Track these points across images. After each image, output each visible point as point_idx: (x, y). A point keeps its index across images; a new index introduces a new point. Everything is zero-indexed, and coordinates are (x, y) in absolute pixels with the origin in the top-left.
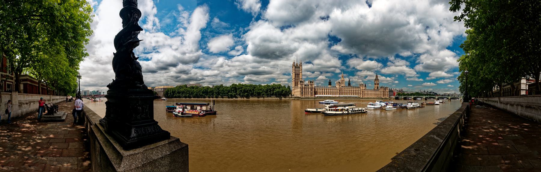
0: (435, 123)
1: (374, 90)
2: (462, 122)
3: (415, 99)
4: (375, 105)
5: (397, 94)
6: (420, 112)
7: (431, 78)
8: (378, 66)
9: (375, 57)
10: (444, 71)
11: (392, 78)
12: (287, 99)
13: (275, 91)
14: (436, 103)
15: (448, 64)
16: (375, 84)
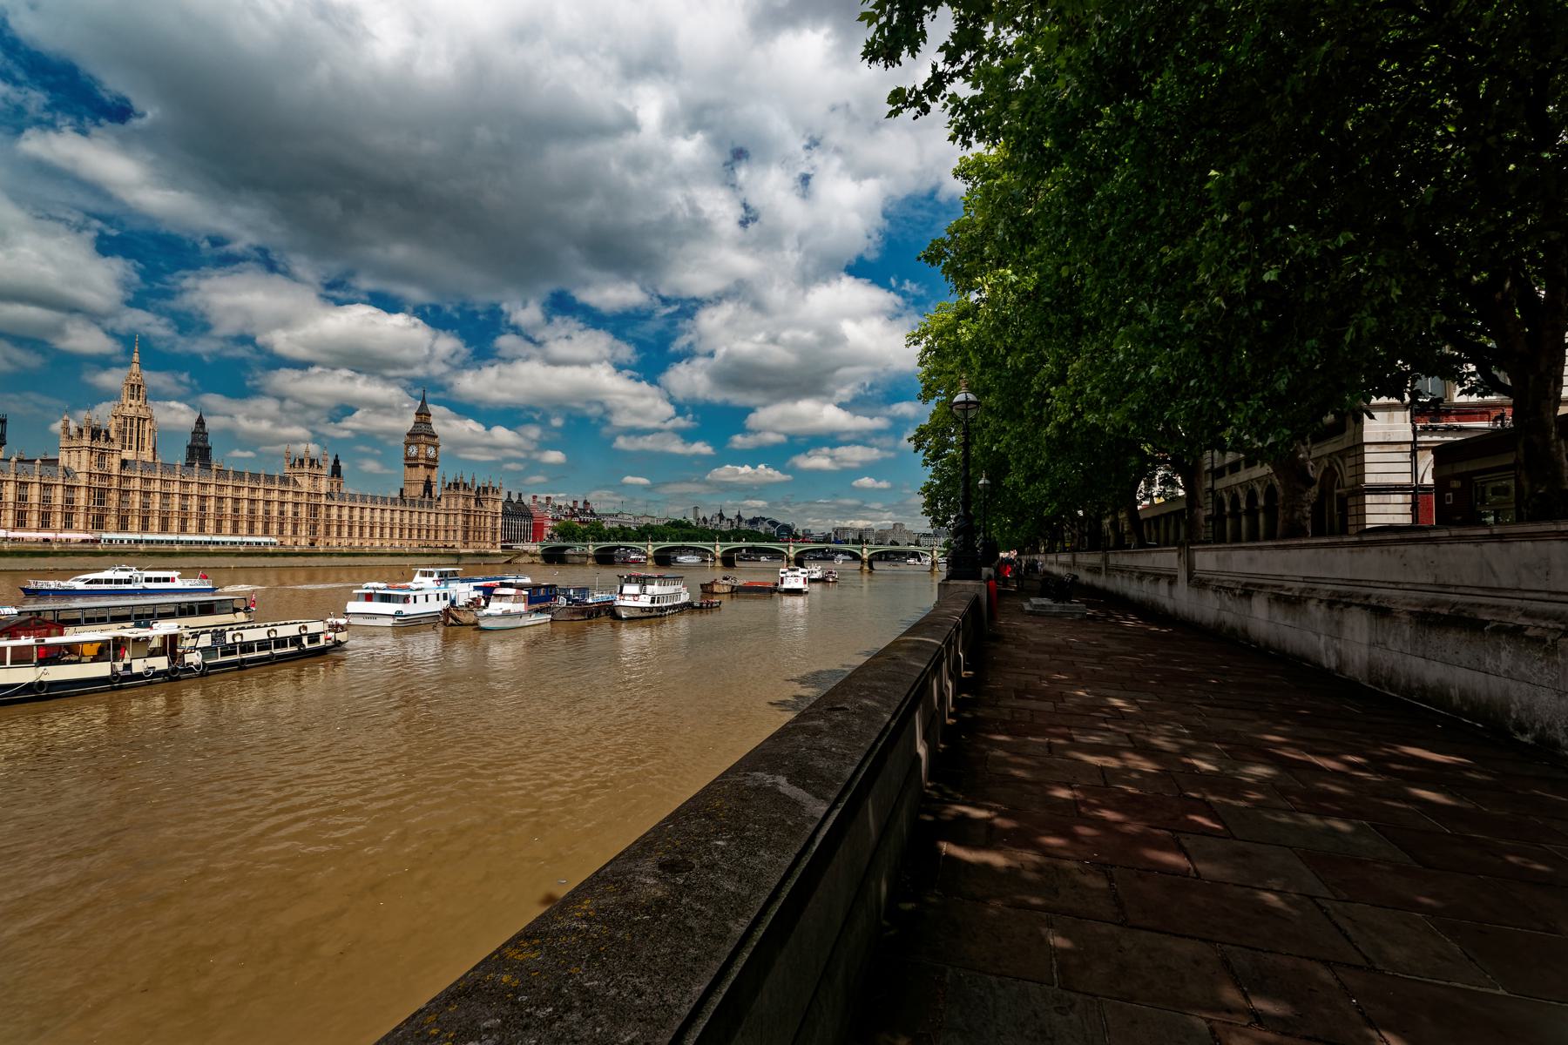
0: (782, 704)
1: (404, 502)
2: (942, 697)
3: (663, 559)
4: (406, 599)
6: (693, 640)
7: (760, 436)
8: (431, 349)
9: (415, 294)
10: (836, 399)
11: (523, 429)
14: (786, 586)
15: (855, 360)
16: (410, 466)
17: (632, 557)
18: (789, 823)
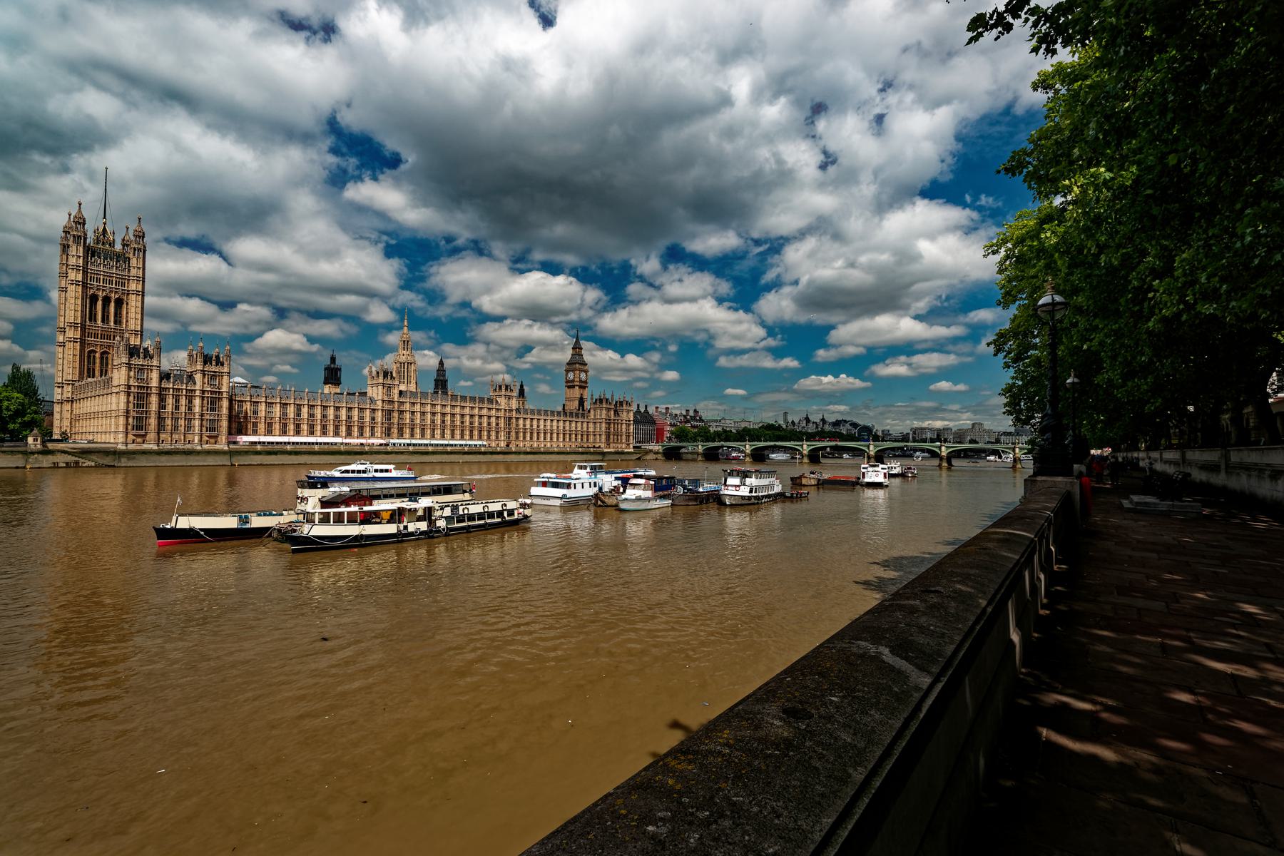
0: (867, 584)
1: (565, 414)
3: (759, 456)
4: (568, 486)
5: (672, 432)
6: (789, 524)
7: (841, 350)
8: (583, 300)
9: (571, 260)
10: (912, 312)
11: (647, 355)
14: (867, 480)
15: (928, 276)
16: (569, 387)
18: (896, 689)
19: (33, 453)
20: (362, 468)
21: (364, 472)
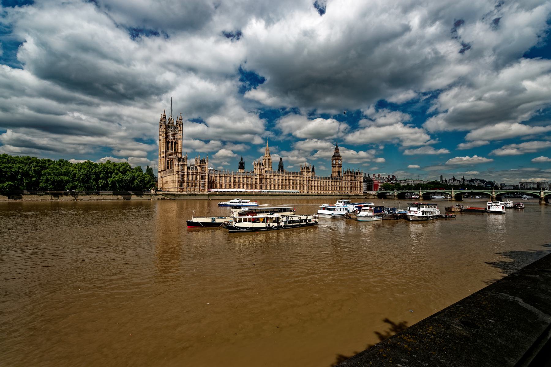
1: (332, 179)
3: (427, 197)
4: (334, 210)
5: (381, 186)
7: (473, 143)
9: (334, 112)
10: (520, 119)
12: (145, 198)
13: (110, 180)
14: (491, 210)
16: (333, 167)
17: (413, 196)
19: (153, 195)
20: (237, 201)
21: (238, 203)
